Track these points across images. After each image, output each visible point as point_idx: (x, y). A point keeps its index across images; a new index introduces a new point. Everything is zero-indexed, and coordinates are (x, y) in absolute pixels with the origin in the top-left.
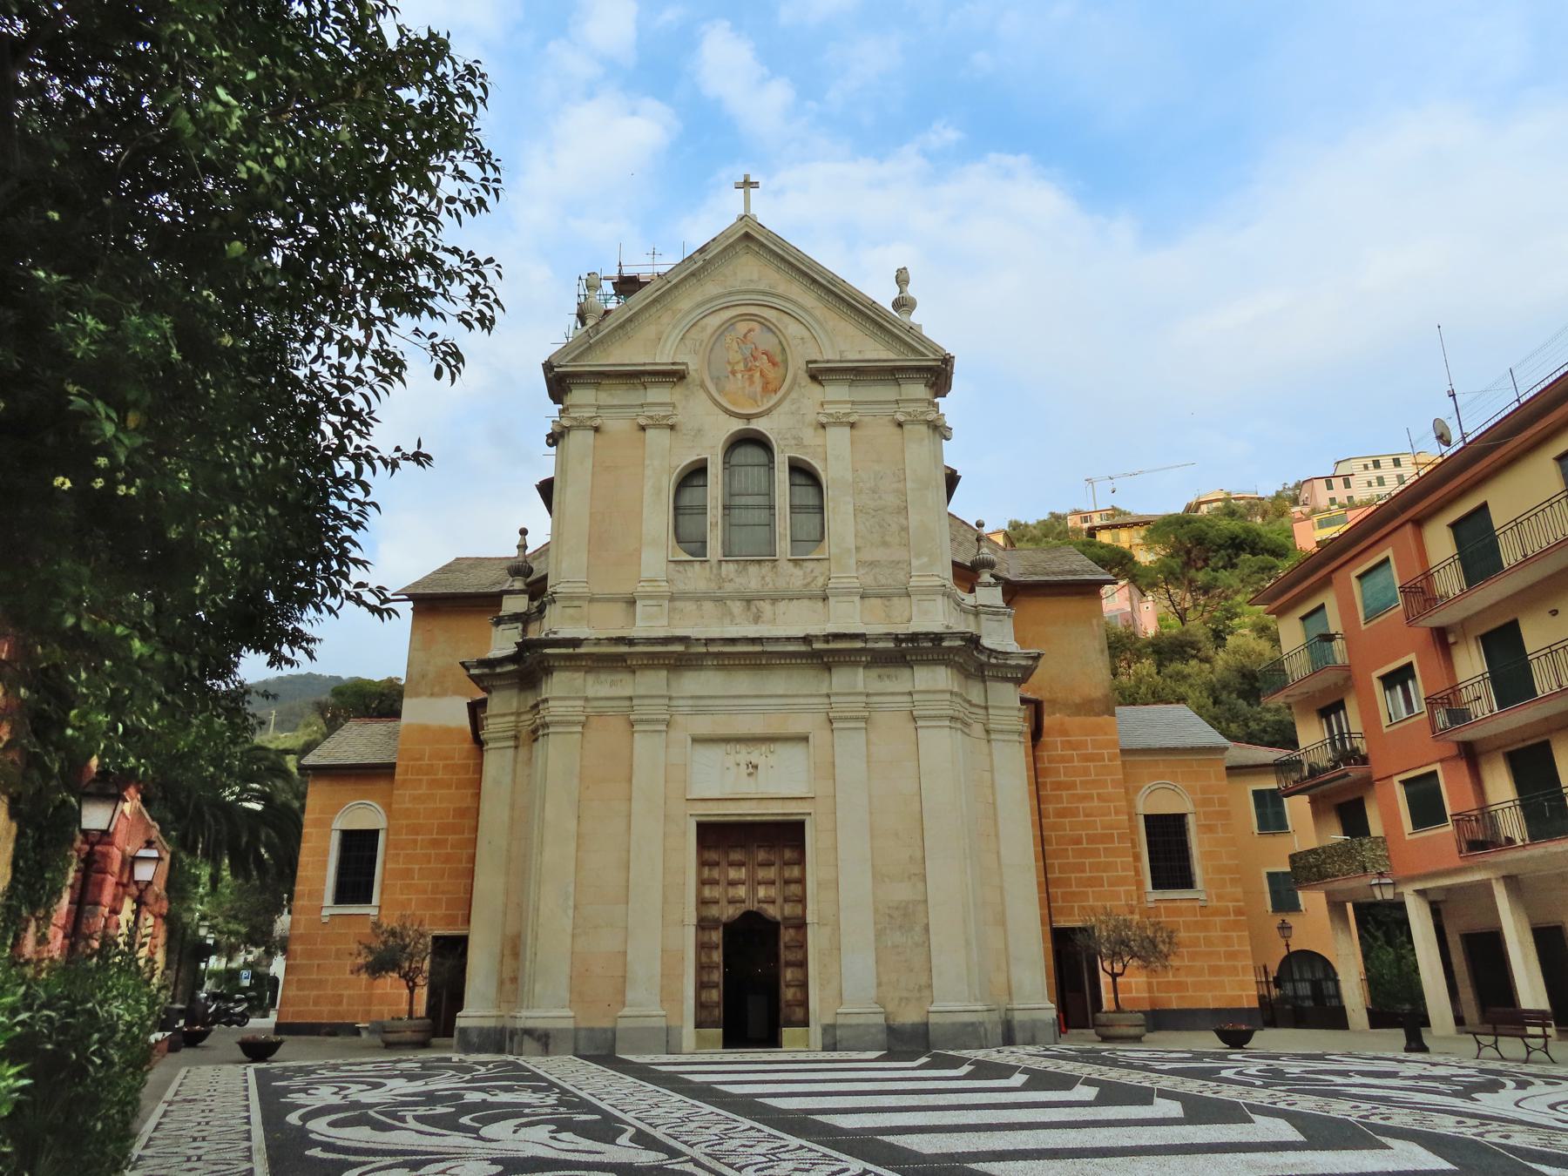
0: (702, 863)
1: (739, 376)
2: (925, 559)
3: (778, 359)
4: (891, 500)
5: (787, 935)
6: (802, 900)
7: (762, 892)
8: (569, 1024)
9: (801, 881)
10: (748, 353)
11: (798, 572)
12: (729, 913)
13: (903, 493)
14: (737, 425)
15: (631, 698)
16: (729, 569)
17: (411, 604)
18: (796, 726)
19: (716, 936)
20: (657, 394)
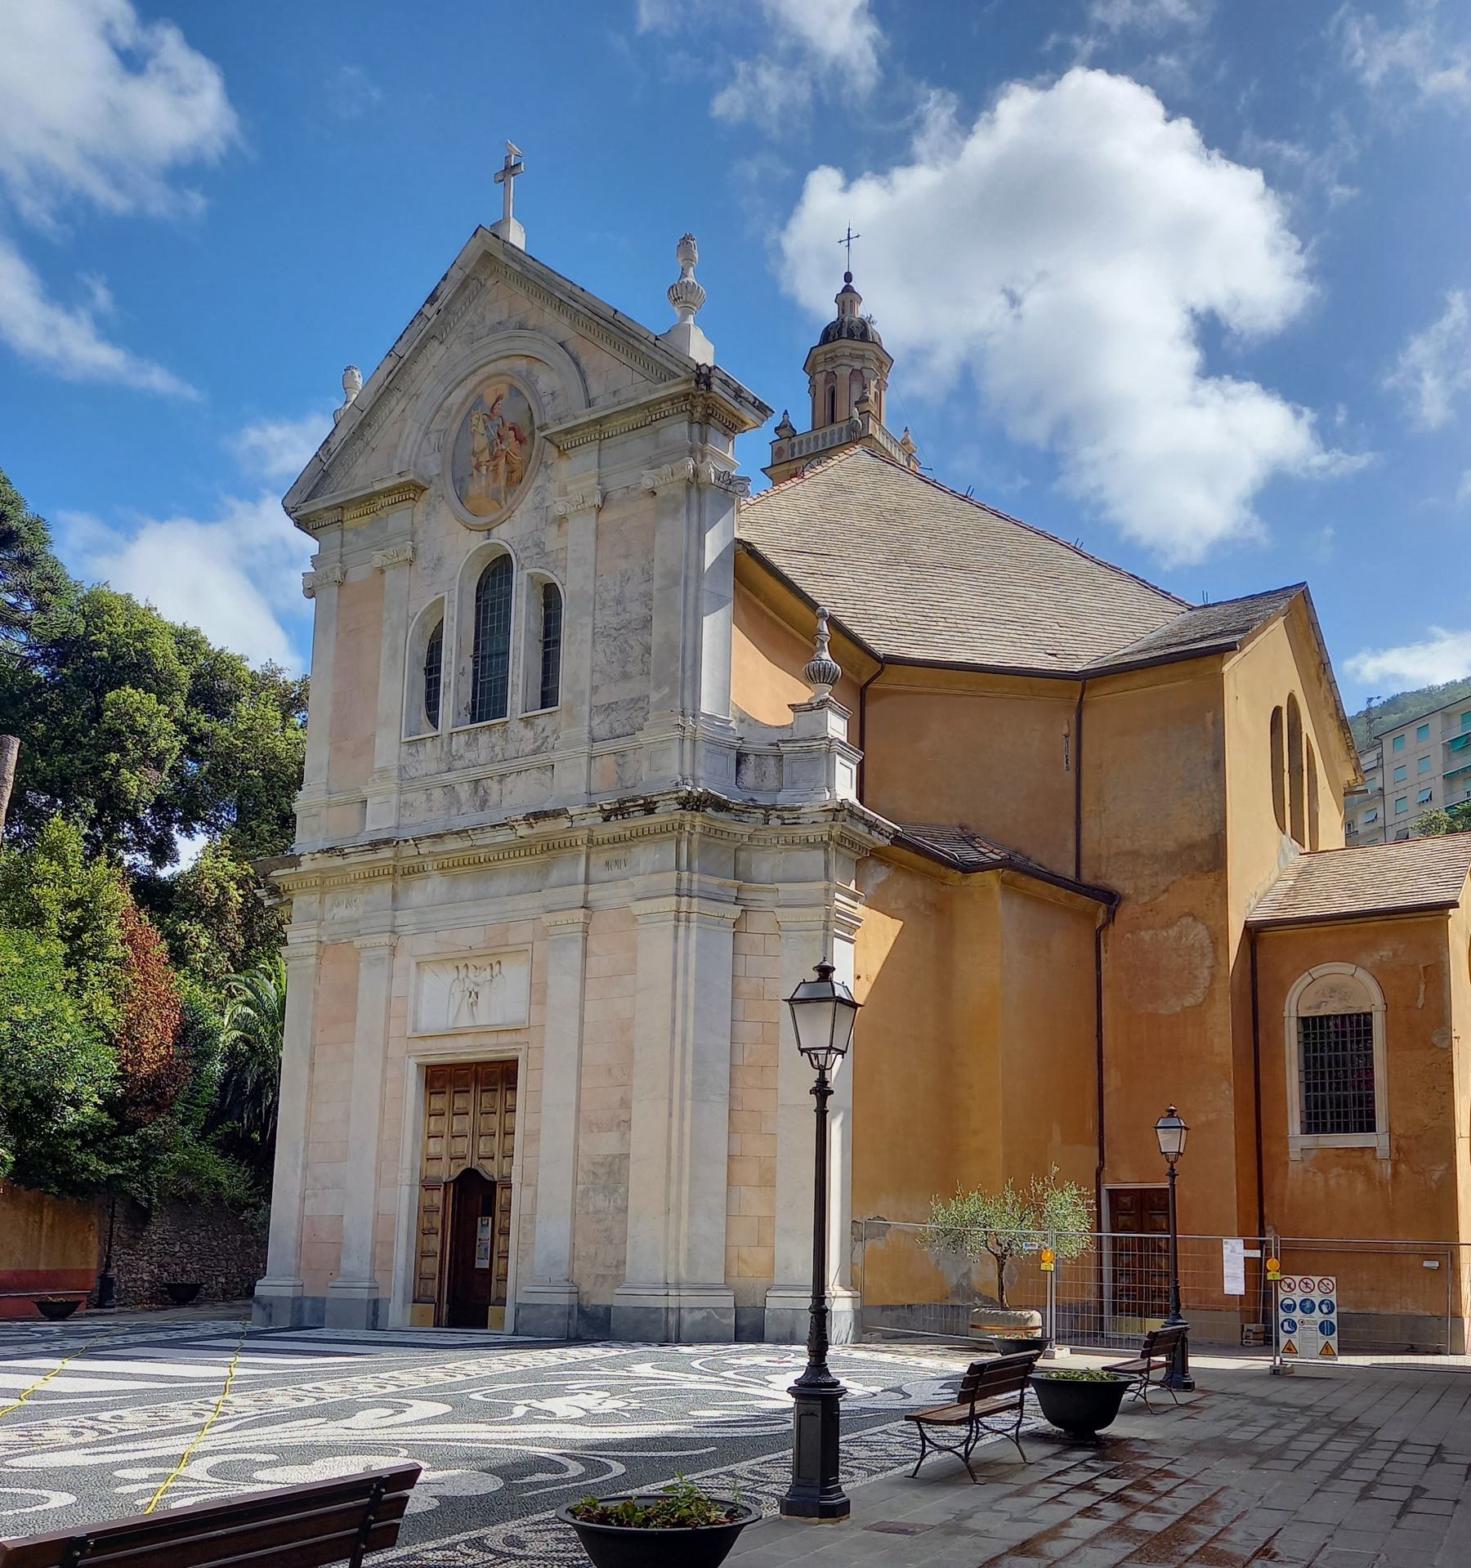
1: (483, 469)
2: (666, 690)
3: (526, 434)
4: (636, 610)
7: (483, 1149)
8: (288, 1292)
11: (529, 734)
12: (447, 1171)
13: (647, 598)
14: (476, 541)
15: (357, 921)
19: (437, 1197)
20: (398, 518)
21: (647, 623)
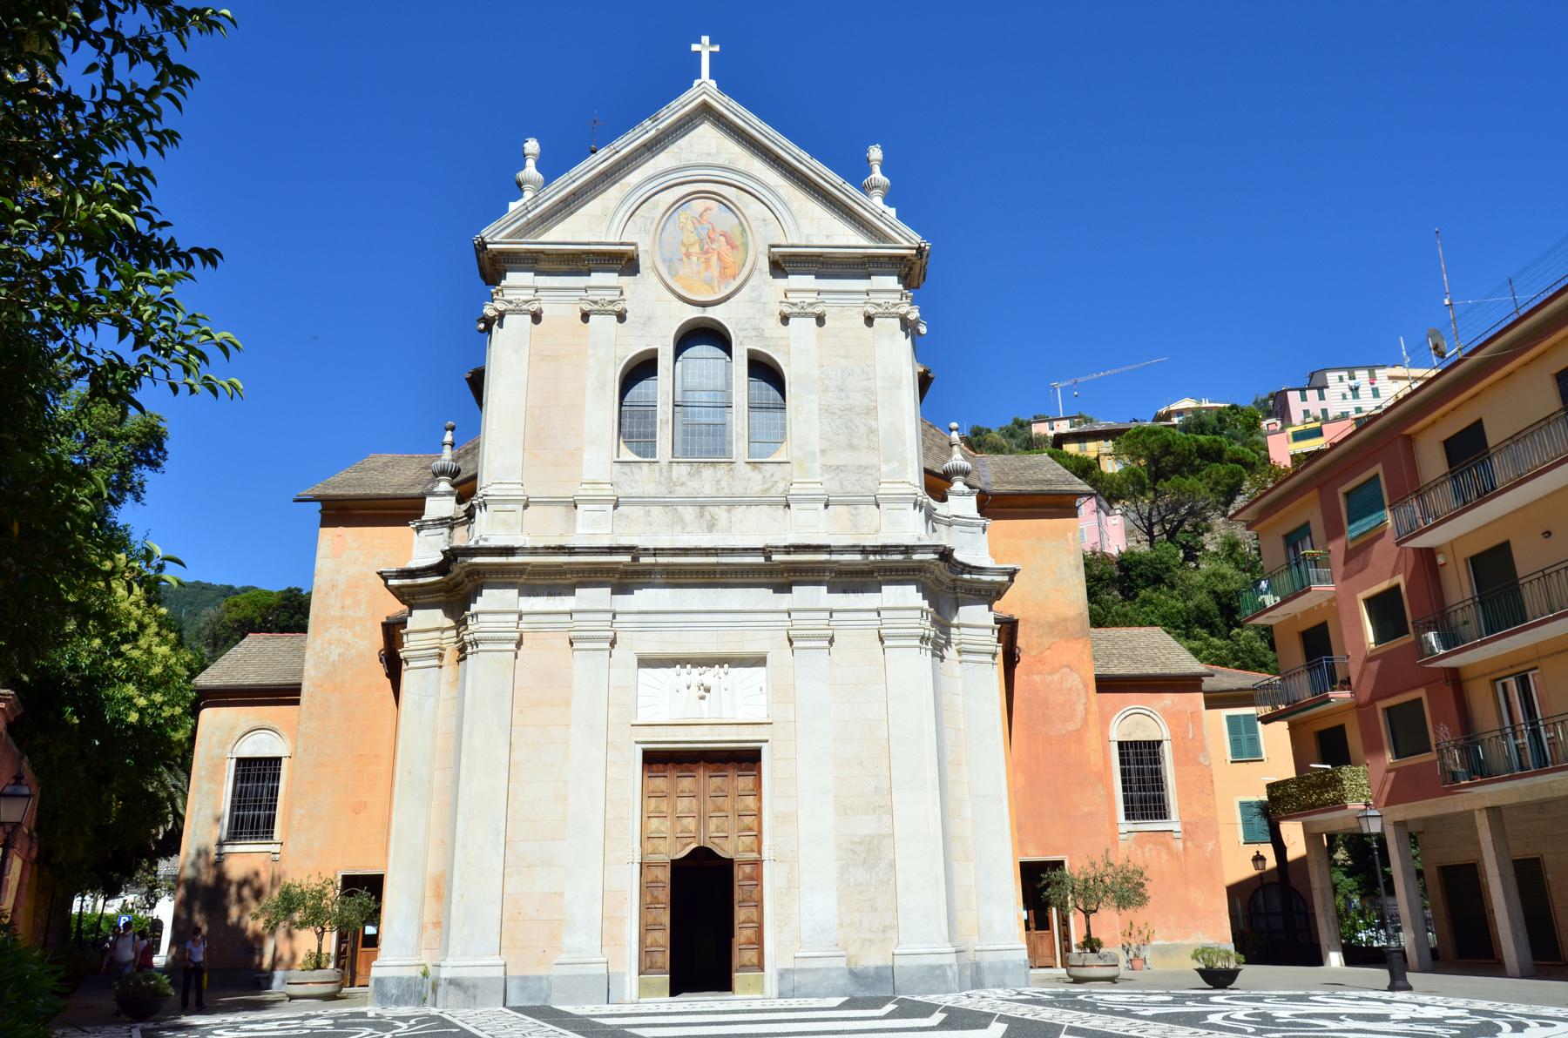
0: (647, 795)
1: (694, 259)
2: (896, 465)
3: (738, 241)
5: (740, 873)
6: (758, 836)
9: (758, 814)
10: (704, 234)
11: (756, 476)
14: (693, 313)
16: (681, 471)
17: (318, 506)
18: (750, 647)
21: (870, 411)
